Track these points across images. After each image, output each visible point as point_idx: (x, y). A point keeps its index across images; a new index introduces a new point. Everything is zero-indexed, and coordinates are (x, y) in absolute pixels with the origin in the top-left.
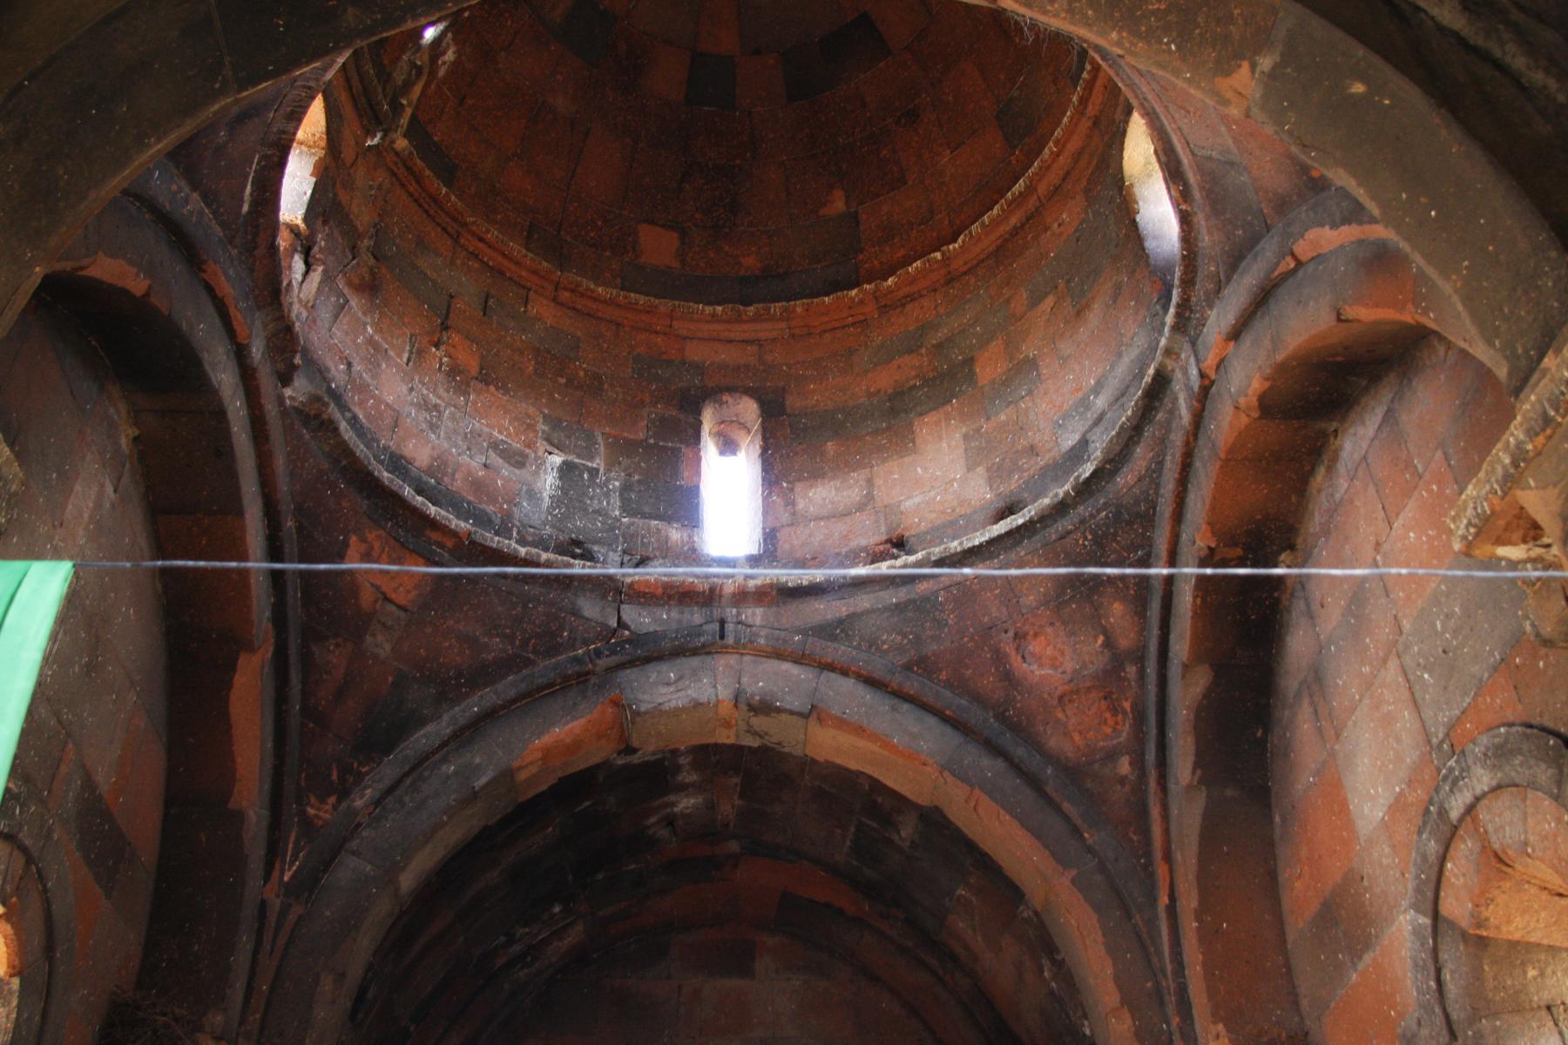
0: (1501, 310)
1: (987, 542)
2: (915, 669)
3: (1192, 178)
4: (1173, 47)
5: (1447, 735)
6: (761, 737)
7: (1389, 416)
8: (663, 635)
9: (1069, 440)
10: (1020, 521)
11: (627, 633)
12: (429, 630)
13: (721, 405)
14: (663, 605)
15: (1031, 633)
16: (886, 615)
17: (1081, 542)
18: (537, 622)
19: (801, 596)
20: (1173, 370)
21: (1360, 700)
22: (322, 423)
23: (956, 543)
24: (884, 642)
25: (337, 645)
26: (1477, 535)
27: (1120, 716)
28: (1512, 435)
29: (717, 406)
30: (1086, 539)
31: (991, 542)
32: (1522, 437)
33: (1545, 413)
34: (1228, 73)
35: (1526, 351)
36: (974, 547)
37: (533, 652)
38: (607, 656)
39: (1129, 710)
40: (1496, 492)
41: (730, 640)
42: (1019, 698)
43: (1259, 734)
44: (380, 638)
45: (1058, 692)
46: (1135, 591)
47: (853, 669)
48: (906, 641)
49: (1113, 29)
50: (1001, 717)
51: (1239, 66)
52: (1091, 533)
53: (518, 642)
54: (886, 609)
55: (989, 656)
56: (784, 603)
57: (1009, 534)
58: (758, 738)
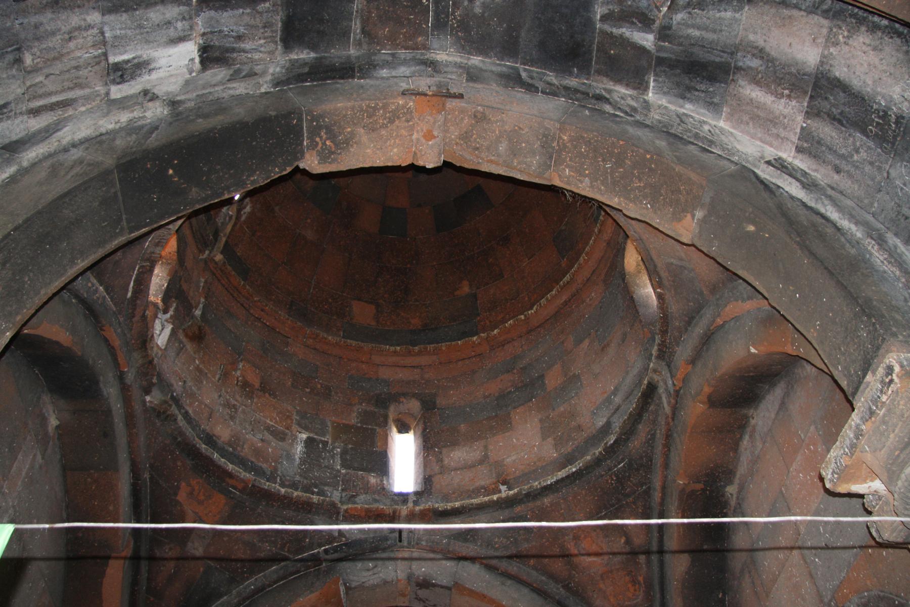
0: (840, 349)
3: (664, 274)
5: (833, 597)
6: (424, 602)
7: (783, 405)
9: (601, 422)
10: (574, 470)
11: (344, 539)
13: (399, 403)
15: (583, 536)
17: (610, 481)
20: (658, 381)
21: (779, 575)
22: (168, 416)
23: (537, 483)
24: (496, 543)
26: (838, 479)
27: (637, 585)
28: (853, 420)
29: (397, 404)
30: (613, 480)
31: (557, 482)
32: (858, 421)
33: (870, 408)
34: (680, 220)
35: (856, 372)
36: (548, 485)
37: (288, 551)
38: (332, 554)
39: (642, 582)
40: (847, 454)
41: (405, 543)
42: (577, 575)
43: (720, 596)
44: (196, 544)
45: (600, 572)
46: (642, 510)
48: (509, 542)
50: (566, 587)
51: (686, 216)
52: (615, 476)
53: (279, 546)
57: (568, 477)
58: (422, 602)
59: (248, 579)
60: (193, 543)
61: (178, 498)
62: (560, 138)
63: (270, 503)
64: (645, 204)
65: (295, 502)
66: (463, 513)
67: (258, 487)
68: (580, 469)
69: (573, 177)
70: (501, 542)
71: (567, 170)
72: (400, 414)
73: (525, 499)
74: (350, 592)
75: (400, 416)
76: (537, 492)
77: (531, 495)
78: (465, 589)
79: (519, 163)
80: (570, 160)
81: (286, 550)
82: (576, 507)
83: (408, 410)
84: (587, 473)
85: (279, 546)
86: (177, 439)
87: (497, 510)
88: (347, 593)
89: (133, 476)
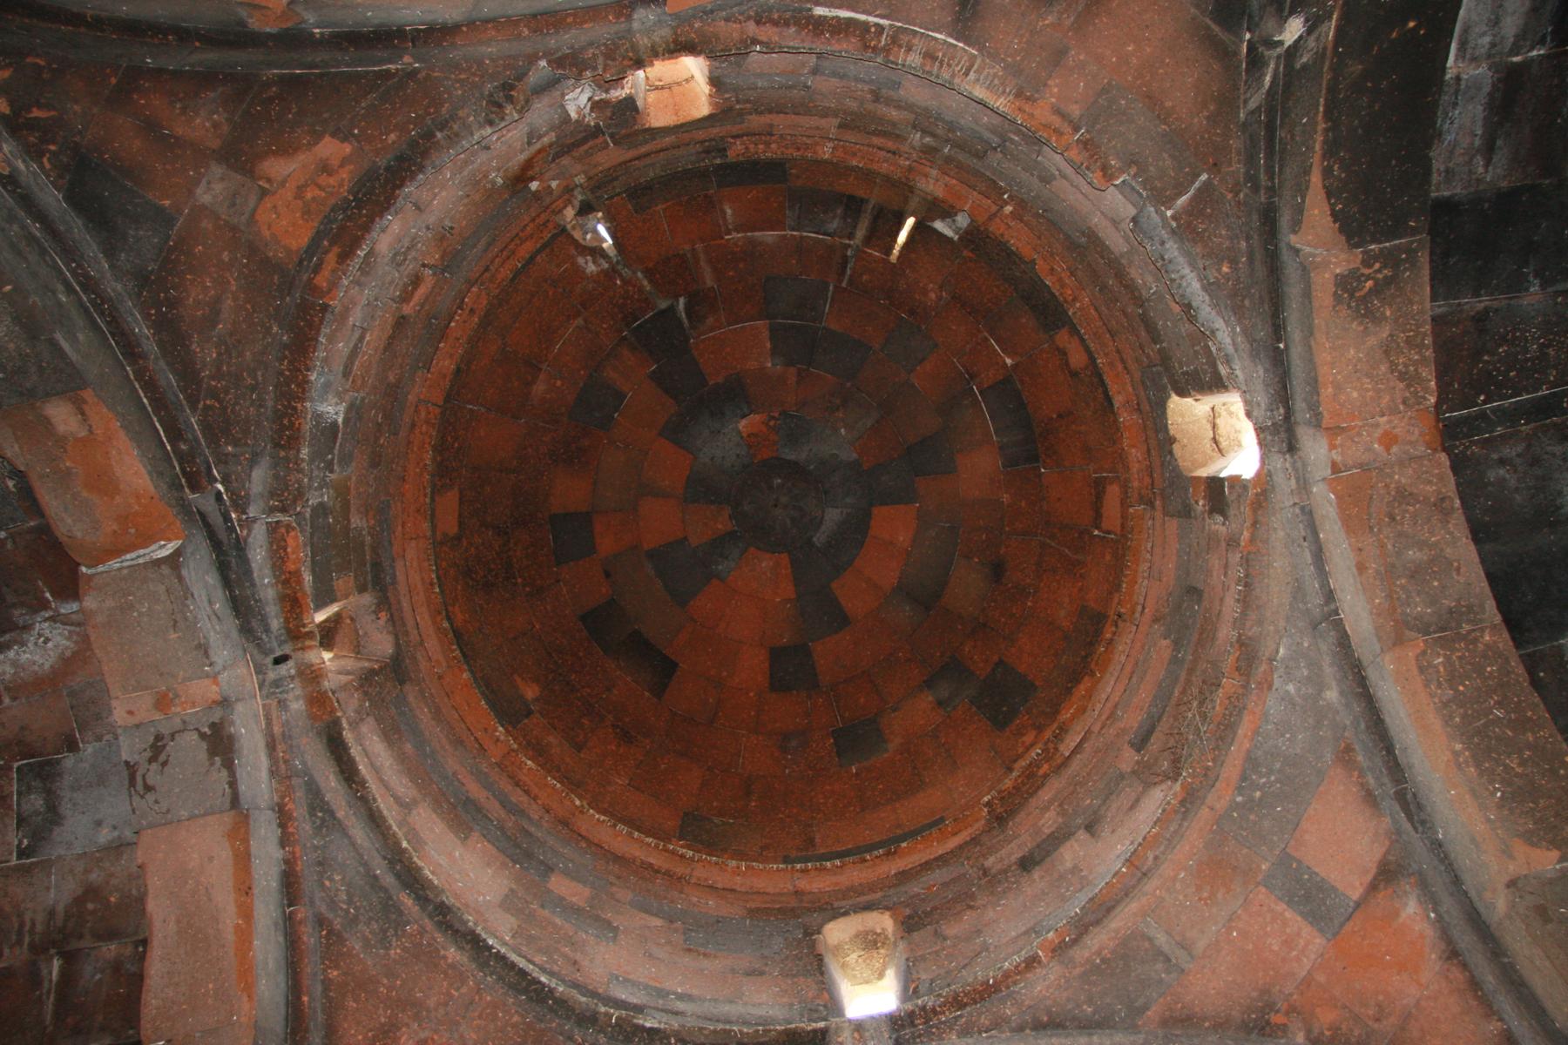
1: (499, 951)
2: (324, 933)
4: (1499, 794)
8: (253, 585)
11: (245, 532)
12: (226, 256)
13: (374, 612)
14: (275, 576)
16: (361, 869)
18: (237, 408)
19: (332, 752)
22: (500, 106)
24: (331, 879)
25: (216, 126)
29: (373, 608)
31: (501, 958)
34: (1533, 845)
36: (485, 940)
37: (206, 408)
38: (220, 510)
44: (218, 187)
47: (297, 849)
48: (345, 907)
49: (1463, 743)
53: (213, 383)
54: (365, 864)
55: (383, 1020)
56: (319, 734)
57: (523, 973)
58: (148, 754)
59: (147, 316)
60: (222, 179)
61: (327, 139)
62: (1482, 630)
63: (287, 353)
64: (1494, 788)
65: (295, 409)
66: (351, 788)
67: (321, 321)
68: (551, 991)
69: (1438, 672)
70: (338, 890)
71: (1440, 660)
72: (352, 619)
73: (431, 908)
74: (165, 570)
75: (348, 621)
76: (457, 925)
77: (445, 916)
78: (246, 841)
79: (1402, 587)
80: (1460, 658)
81: (208, 402)
82: (480, 1017)
83: (366, 633)
84: (551, 1009)
85: (213, 383)
86: (441, 130)
87: (385, 858)
88: (158, 563)
89: (418, 31)
